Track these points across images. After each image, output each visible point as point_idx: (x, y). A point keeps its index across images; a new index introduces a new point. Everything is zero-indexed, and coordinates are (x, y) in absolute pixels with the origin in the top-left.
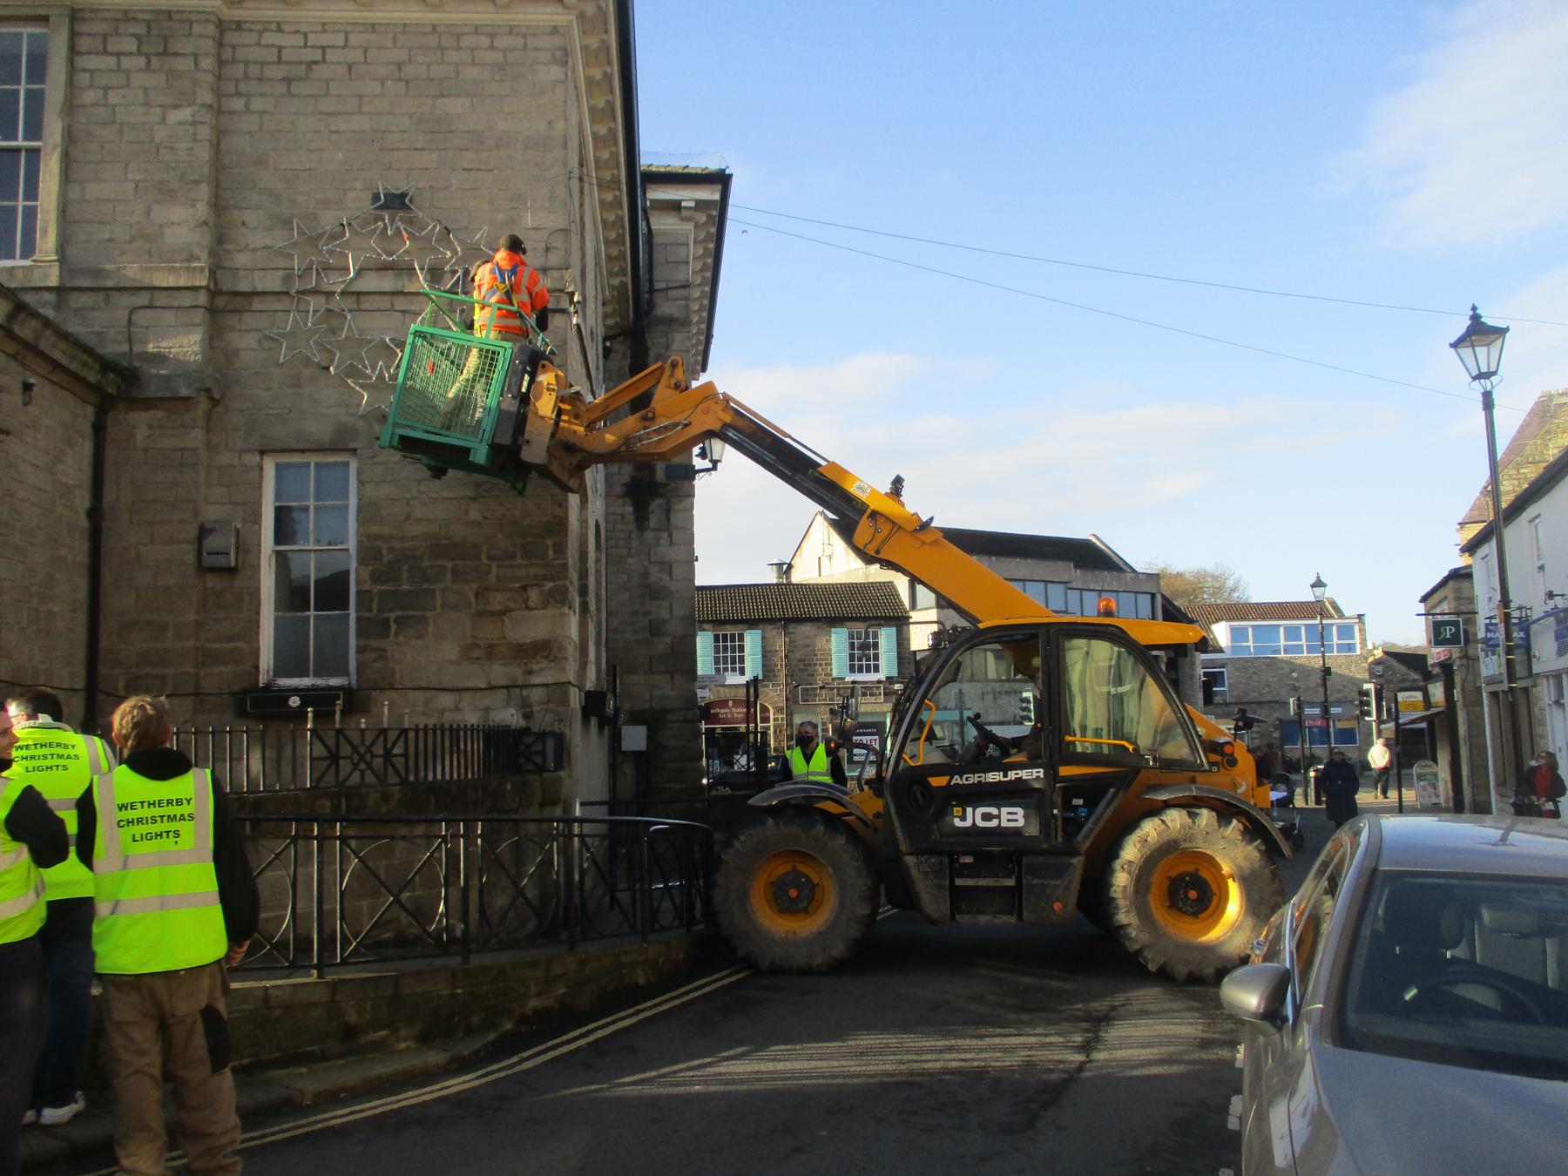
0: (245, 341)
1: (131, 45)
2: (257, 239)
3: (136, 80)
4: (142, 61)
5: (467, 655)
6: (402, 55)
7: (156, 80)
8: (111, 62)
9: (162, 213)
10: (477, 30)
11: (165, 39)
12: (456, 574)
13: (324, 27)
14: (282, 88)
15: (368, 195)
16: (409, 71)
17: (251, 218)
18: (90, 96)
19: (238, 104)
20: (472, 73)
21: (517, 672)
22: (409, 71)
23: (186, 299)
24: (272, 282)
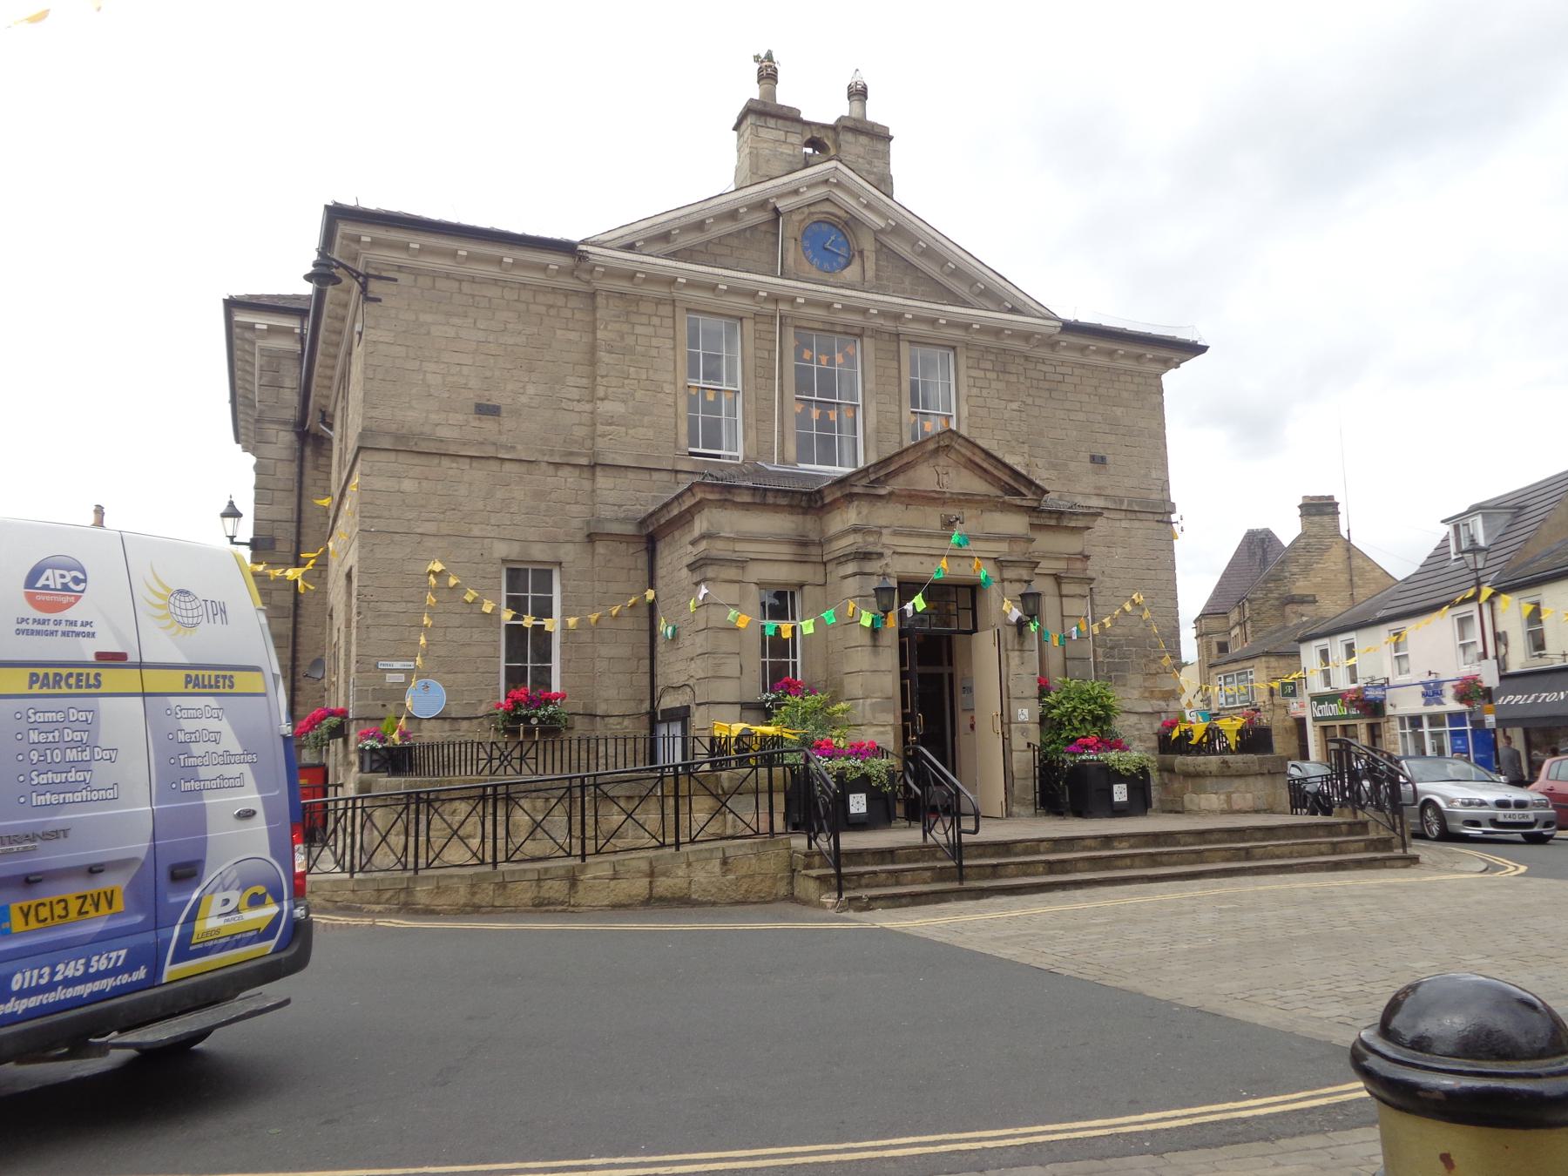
1: (989, 365)
3: (994, 384)
4: (994, 376)
7: (1001, 385)
8: (981, 374)
11: (1004, 364)
13: (1063, 363)
14: (1046, 394)
15: (1087, 455)
16: (1101, 391)
19: (1029, 401)
20: (1125, 395)
21: (1163, 704)
22: (1101, 391)
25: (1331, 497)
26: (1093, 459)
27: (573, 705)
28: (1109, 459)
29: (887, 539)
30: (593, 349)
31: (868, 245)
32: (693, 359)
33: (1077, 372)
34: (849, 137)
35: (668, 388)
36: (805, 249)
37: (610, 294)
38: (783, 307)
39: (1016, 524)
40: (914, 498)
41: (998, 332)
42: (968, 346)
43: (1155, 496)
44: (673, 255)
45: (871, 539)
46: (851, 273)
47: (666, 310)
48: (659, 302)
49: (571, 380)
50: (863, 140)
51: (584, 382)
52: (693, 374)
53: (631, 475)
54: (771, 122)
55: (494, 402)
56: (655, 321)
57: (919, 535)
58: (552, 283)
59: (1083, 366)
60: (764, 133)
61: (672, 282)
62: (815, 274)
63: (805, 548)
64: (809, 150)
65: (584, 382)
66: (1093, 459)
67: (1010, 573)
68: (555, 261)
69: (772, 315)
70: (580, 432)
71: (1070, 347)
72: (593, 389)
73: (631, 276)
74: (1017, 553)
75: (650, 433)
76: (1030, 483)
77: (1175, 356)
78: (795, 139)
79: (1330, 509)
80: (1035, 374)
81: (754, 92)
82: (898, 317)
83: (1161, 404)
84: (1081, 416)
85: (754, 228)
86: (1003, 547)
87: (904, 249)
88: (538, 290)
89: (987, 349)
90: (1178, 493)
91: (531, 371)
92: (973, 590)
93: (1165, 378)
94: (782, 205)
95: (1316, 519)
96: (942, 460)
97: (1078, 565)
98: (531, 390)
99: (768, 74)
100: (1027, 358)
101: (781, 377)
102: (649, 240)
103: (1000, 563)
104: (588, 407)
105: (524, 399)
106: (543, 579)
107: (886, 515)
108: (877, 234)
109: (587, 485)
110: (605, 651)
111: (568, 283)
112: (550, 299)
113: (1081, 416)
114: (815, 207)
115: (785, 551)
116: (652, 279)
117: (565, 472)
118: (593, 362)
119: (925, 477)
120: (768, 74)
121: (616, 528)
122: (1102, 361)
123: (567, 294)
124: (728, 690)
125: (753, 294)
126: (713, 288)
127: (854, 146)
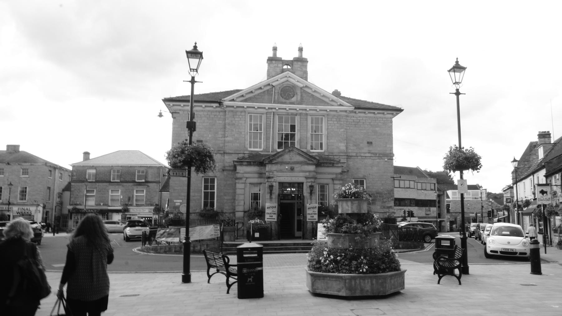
0: (351, 163)
1: (335, 120)
2: (352, 148)
5: (381, 208)
6: (370, 121)
9: (340, 144)
10: (380, 118)
12: (380, 197)
13: (360, 117)
17: (351, 145)
18: (330, 127)
19: (348, 128)
23: (344, 157)
24: (354, 154)
25: (548, 132)
26: (368, 143)
27: (219, 211)
28: (373, 143)
29: (275, 173)
30: (225, 124)
31: (299, 92)
32: (251, 125)
33: (364, 119)
34: (295, 63)
35: (243, 133)
36: (281, 94)
37: (230, 111)
38: (274, 110)
39: (312, 168)
40: (282, 163)
41: (336, 111)
42: (328, 115)
43: (388, 152)
44: (246, 101)
45: (271, 173)
46: (294, 99)
47: (243, 114)
48: (241, 112)
49: (220, 133)
50: (299, 63)
51: (223, 133)
52: (251, 130)
53: (233, 155)
54: (274, 62)
55: (201, 139)
56: (241, 117)
57: (283, 172)
58: (215, 110)
59: (366, 117)
60: (272, 66)
61: (243, 107)
62: (284, 100)
63: (261, 175)
64: (285, 67)
65: (223, 133)
66: (368, 143)
67: (309, 180)
68: (215, 105)
69: (271, 113)
70: (221, 145)
71: (359, 112)
72: (225, 134)
73: (233, 107)
74: (312, 174)
75: (238, 145)
76: (315, 158)
77: (395, 113)
78: (280, 65)
79: (548, 136)
80: (351, 121)
81: (271, 55)
82: (306, 110)
83: (392, 126)
84: (365, 131)
85: (268, 90)
86: (307, 174)
87: (309, 91)
88: (212, 112)
89: (334, 116)
90: (395, 151)
91: (210, 131)
92: (303, 183)
93: (393, 119)
94: (274, 84)
95: (543, 139)
96: (292, 153)
97: (339, 176)
98: (210, 136)
99: (275, 49)
100: (348, 116)
101: (273, 128)
102: (237, 98)
103: (307, 178)
104: (223, 139)
105: (208, 138)
106: (213, 181)
107: (274, 167)
108: (301, 88)
109: (223, 158)
110: (226, 198)
111: (219, 109)
112: (215, 113)
113: (365, 131)
114: (286, 81)
115: (256, 175)
116: (237, 107)
117: (218, 155)
118: (225, 128)
119: (287, 157)
120: (275, 49)
121: (229, 168)
122: (372, 115)
123: (219, 112)
124: (241, 208)
125: (265, 108)
126: (254, 107)
127: (297, 65)
